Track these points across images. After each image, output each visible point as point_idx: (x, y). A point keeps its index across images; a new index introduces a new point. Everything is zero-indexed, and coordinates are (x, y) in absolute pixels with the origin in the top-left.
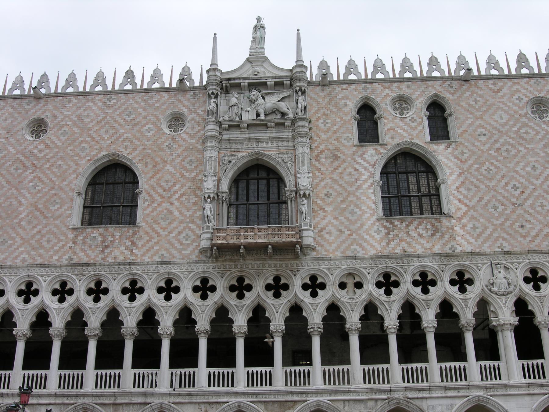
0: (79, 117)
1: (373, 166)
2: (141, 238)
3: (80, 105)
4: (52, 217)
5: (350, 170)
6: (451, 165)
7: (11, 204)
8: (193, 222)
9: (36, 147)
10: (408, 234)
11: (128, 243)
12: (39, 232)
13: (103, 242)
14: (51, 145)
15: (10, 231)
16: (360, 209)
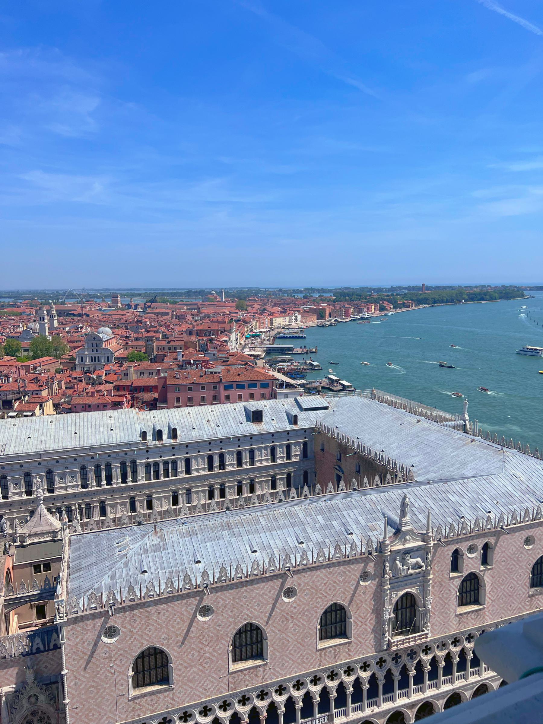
0: (313, 582)
1: (457, 587)
2: (353, 646)
3: (313, 574)
4: (307, 645)
5: (447, 591)
6: (488, 580)
7: (283, 643)
8: (377, 633)
9: (291, 606)
10: (467, 619)
11: (347, 650)
12: (301, 655)
13: (335, 653)
14: (300, 603)
15: (285, 658)
16: (449, 610)
